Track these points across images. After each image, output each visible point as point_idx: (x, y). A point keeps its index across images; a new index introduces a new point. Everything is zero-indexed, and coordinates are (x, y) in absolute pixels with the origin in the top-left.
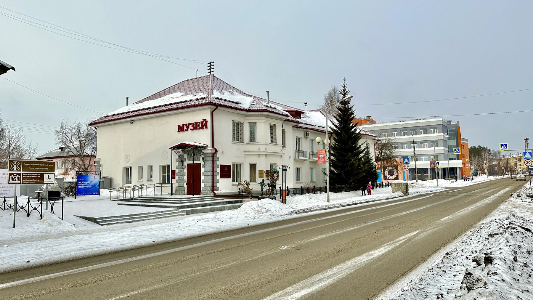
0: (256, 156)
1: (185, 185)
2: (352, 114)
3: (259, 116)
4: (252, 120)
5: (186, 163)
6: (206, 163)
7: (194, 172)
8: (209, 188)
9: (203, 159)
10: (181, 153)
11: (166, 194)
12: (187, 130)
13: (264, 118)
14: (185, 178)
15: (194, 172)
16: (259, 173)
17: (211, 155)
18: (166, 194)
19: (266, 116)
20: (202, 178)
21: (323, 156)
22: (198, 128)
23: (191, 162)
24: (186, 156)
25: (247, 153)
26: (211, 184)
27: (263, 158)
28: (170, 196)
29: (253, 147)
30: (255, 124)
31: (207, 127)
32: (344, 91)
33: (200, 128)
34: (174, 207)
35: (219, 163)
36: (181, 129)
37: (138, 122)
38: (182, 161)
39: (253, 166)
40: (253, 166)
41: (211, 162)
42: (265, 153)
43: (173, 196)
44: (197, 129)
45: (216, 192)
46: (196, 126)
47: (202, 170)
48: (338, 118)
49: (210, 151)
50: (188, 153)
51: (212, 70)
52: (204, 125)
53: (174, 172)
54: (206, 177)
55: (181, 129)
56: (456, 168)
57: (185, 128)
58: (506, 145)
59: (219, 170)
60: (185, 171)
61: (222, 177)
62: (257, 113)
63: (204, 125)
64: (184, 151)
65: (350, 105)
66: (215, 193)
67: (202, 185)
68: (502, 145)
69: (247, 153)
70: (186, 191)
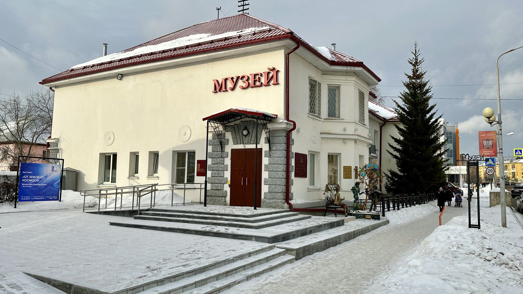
0: (341, 142)
1: (227, 188)
2: (427, 91)
3: (347, 73)
4: (335, 80)
5: (228, 149)
6: (274, 148)
7: (247, 166)
8: (281, 196)
9: (269, 141)
10: (221, 128)
11: (192, 203)
12: (233, 89)
13: (354, 78)
14: (228, 174)
15: (247, 166)
16: (344, 169)
17: (284, 134)
18: (192, 203)
19: (356, 74)
20: (265, 175)
21: (490, 143)
22: (258, 84)
23: (241, 146)
24: (229, 135)
25: (326, 136)
26: (283, 188)
27: (351, 145)
28: (201, 208)
29: (334, 127)
30: (338, 87)
31: (277, 83)
32: (416, 59)
33: (261, 85)
34: (258, 239)
35: (295, 149)
36: (219, 87)
37: (131, 78)
38: (222, 144)
39: (333, 159)
40: (333, 159)
41: (284, 146)
42: (356, 137)
43: (211, 208)
44: (255, 86)
45: (292, 202)
46: (254, 82)
47: (265, 161)
48: (403, 97)
49: (284, 126)
50: (236, 130)
51: (245, 7)
52: (271, 77)
53: (203, 164)
54: (273, 174)
55: (219, 87)
56: (459, 175)
57: (230, 85)
58: (521, 151)
59: (293, 162)
60: (228, 161)
61: (296, 175)
62: (345, 68)
63: (271, 77)
64: (226, 128)
65: (425, 79)
66: (290, 206)
67: (265, 189)
68: (516, 151)
69: (326, 136)
70: (228, 199)
